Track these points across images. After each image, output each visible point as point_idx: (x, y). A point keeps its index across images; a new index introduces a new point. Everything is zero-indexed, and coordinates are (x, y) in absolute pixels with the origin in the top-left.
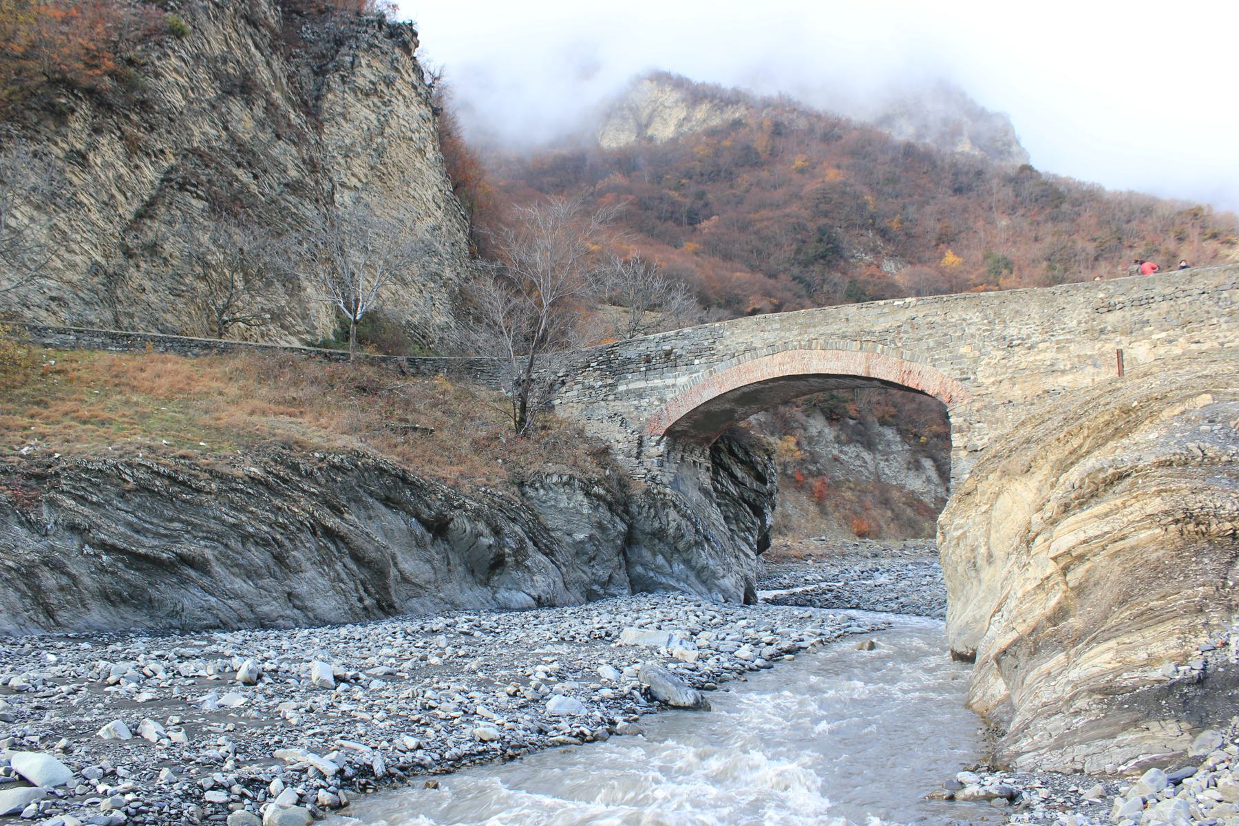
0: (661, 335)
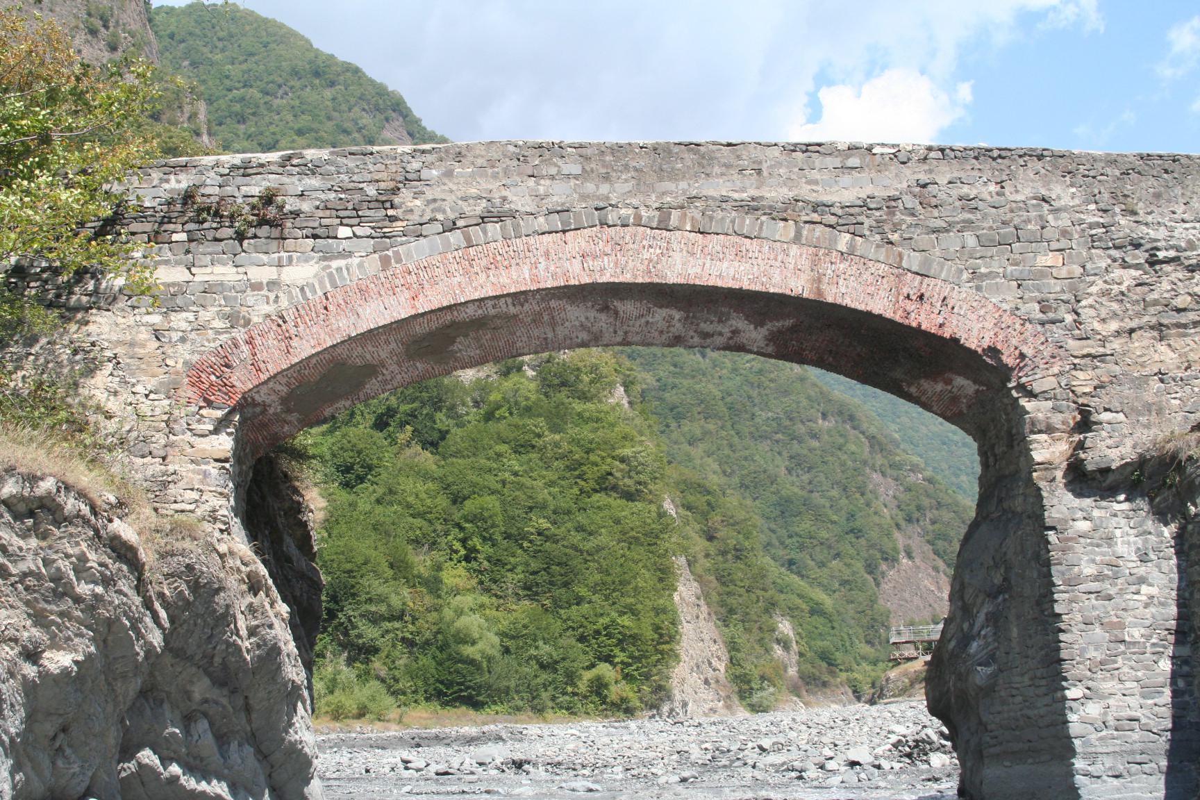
0: (237, 159)
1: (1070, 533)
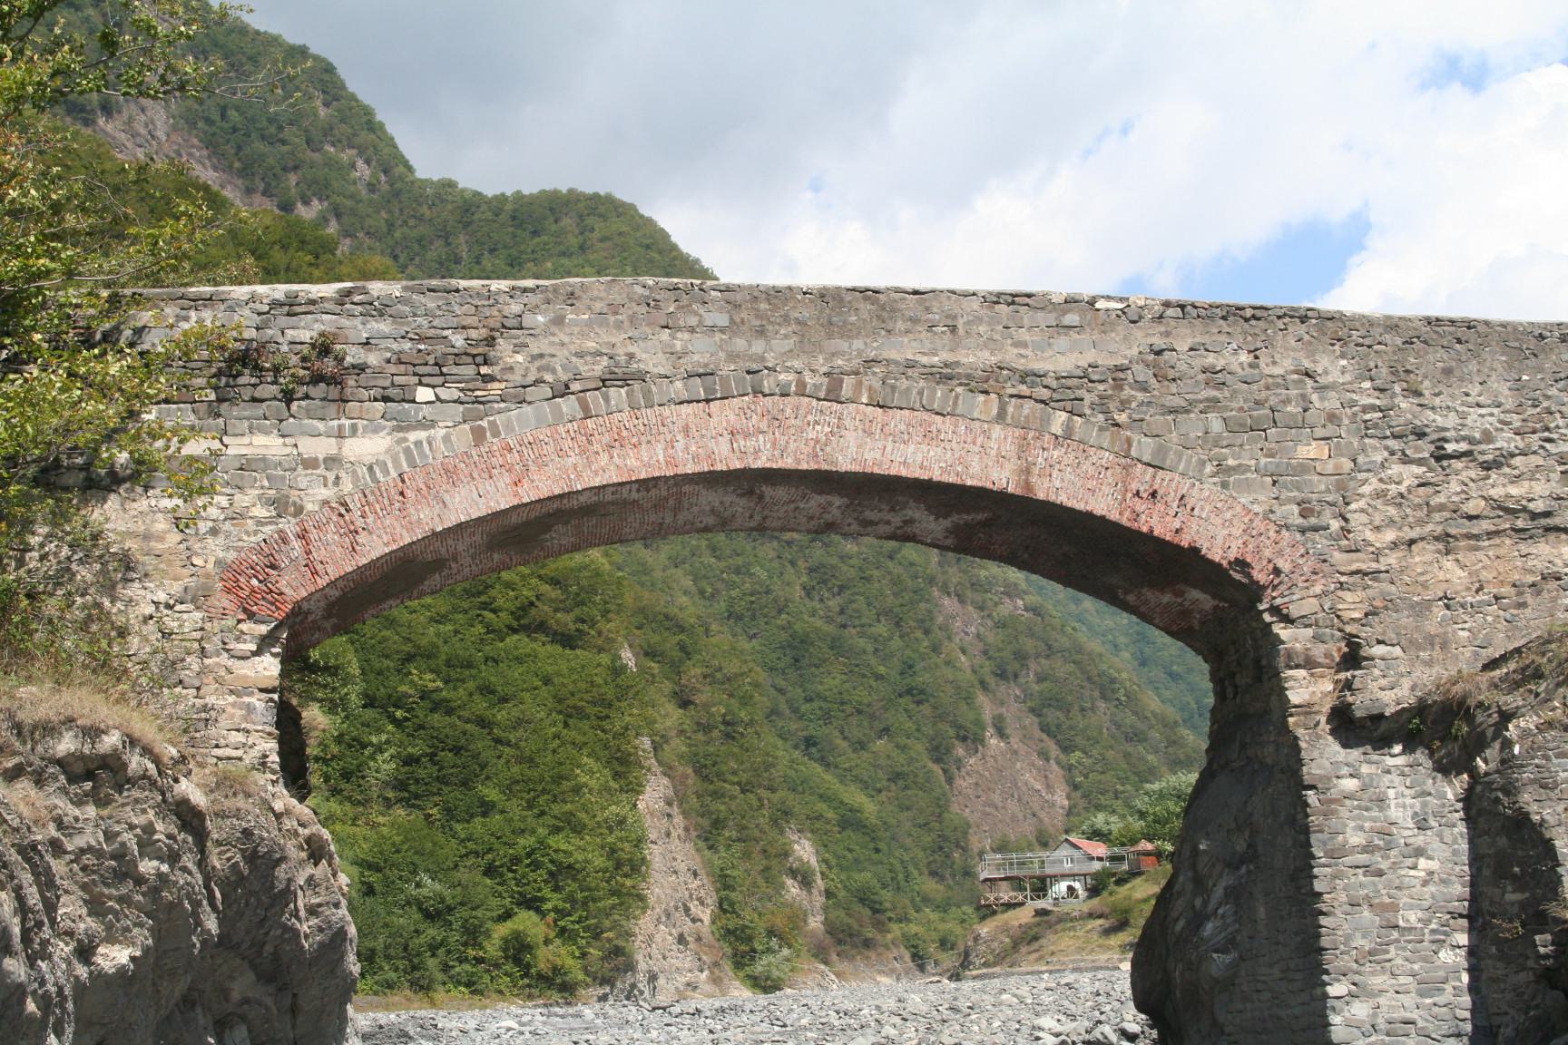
1: (1333, 794)
